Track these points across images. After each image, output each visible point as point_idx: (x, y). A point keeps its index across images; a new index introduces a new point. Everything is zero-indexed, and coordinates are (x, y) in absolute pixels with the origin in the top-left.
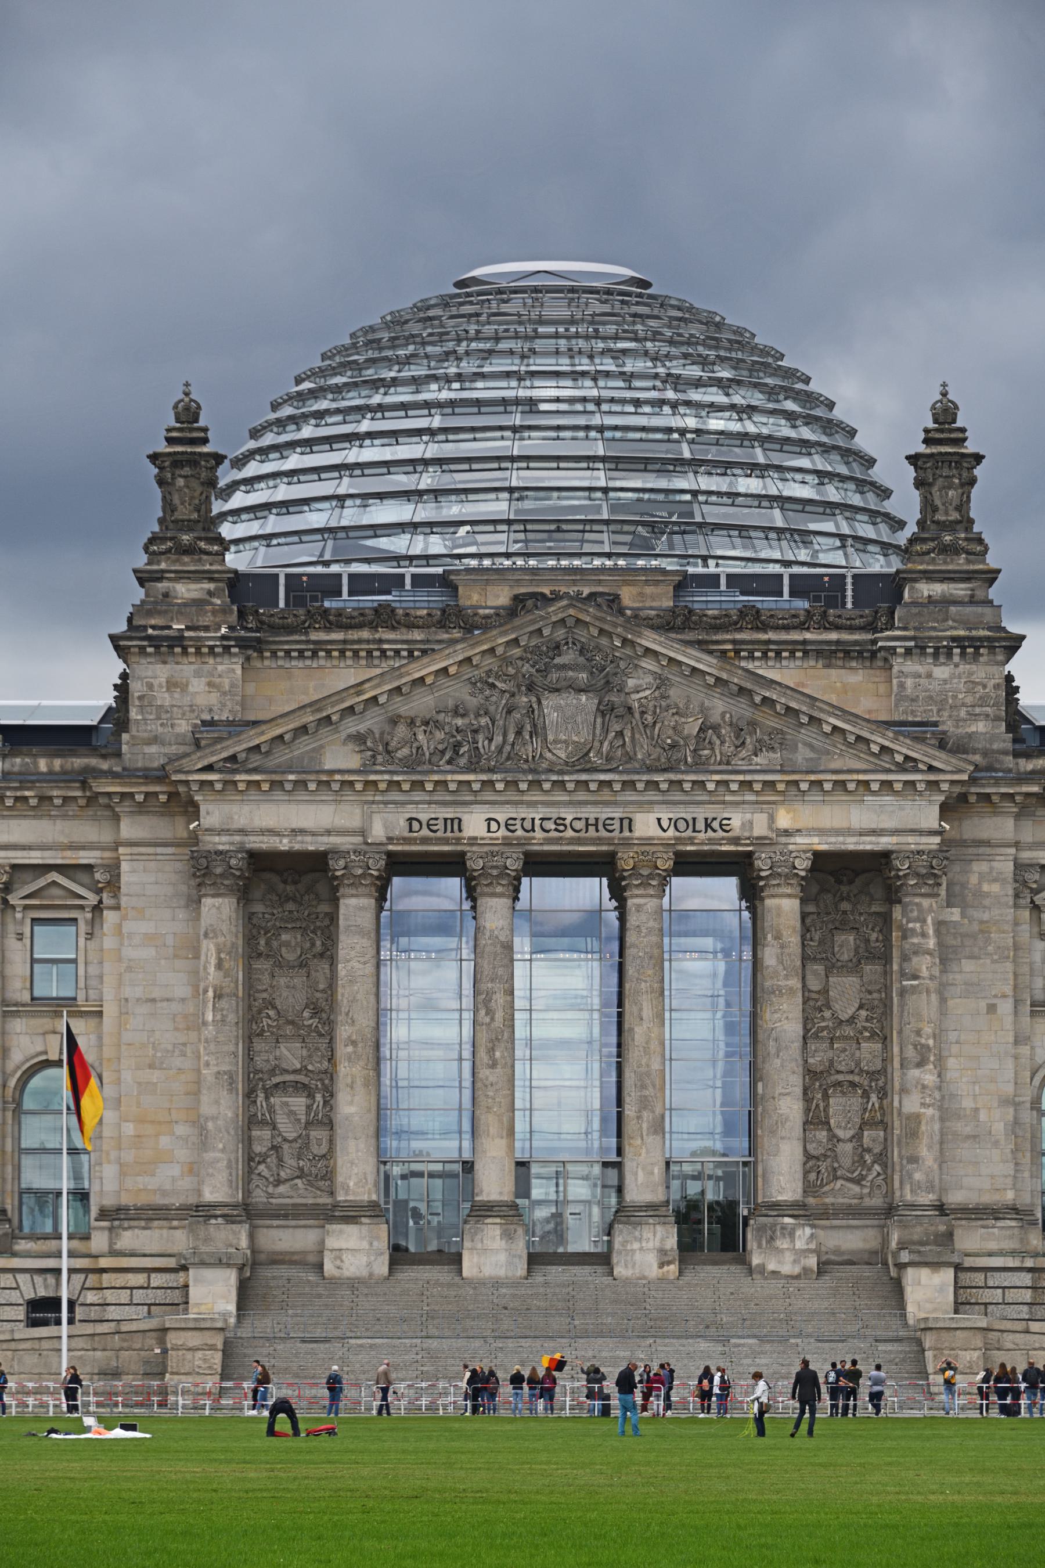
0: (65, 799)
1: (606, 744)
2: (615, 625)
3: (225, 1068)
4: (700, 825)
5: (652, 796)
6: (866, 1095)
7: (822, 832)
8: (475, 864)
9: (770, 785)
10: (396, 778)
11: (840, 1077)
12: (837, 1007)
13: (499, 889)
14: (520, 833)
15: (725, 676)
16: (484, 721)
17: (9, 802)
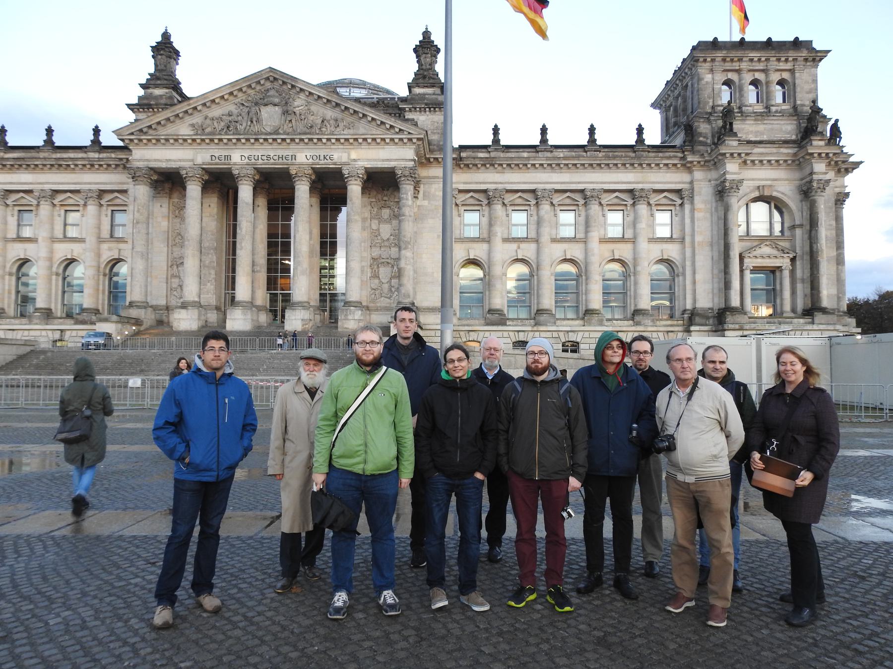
0: (117, 165)
1: (285, 127)
2: (288, 79)
3: (139, 250)
4: (322, 158)
5: (302, 146)
6: (393, 266)
7: (368, 160)
8: (235, 172)
9: (347, 140)
10: (203, 137)
11: (383, 260)
12: (382, 235)
13: (245, 182)
14: (253, 161)
15: (330, 98)
16: (240, 118)
17: (97, 166)
